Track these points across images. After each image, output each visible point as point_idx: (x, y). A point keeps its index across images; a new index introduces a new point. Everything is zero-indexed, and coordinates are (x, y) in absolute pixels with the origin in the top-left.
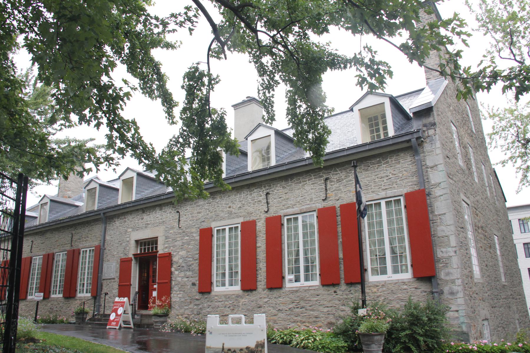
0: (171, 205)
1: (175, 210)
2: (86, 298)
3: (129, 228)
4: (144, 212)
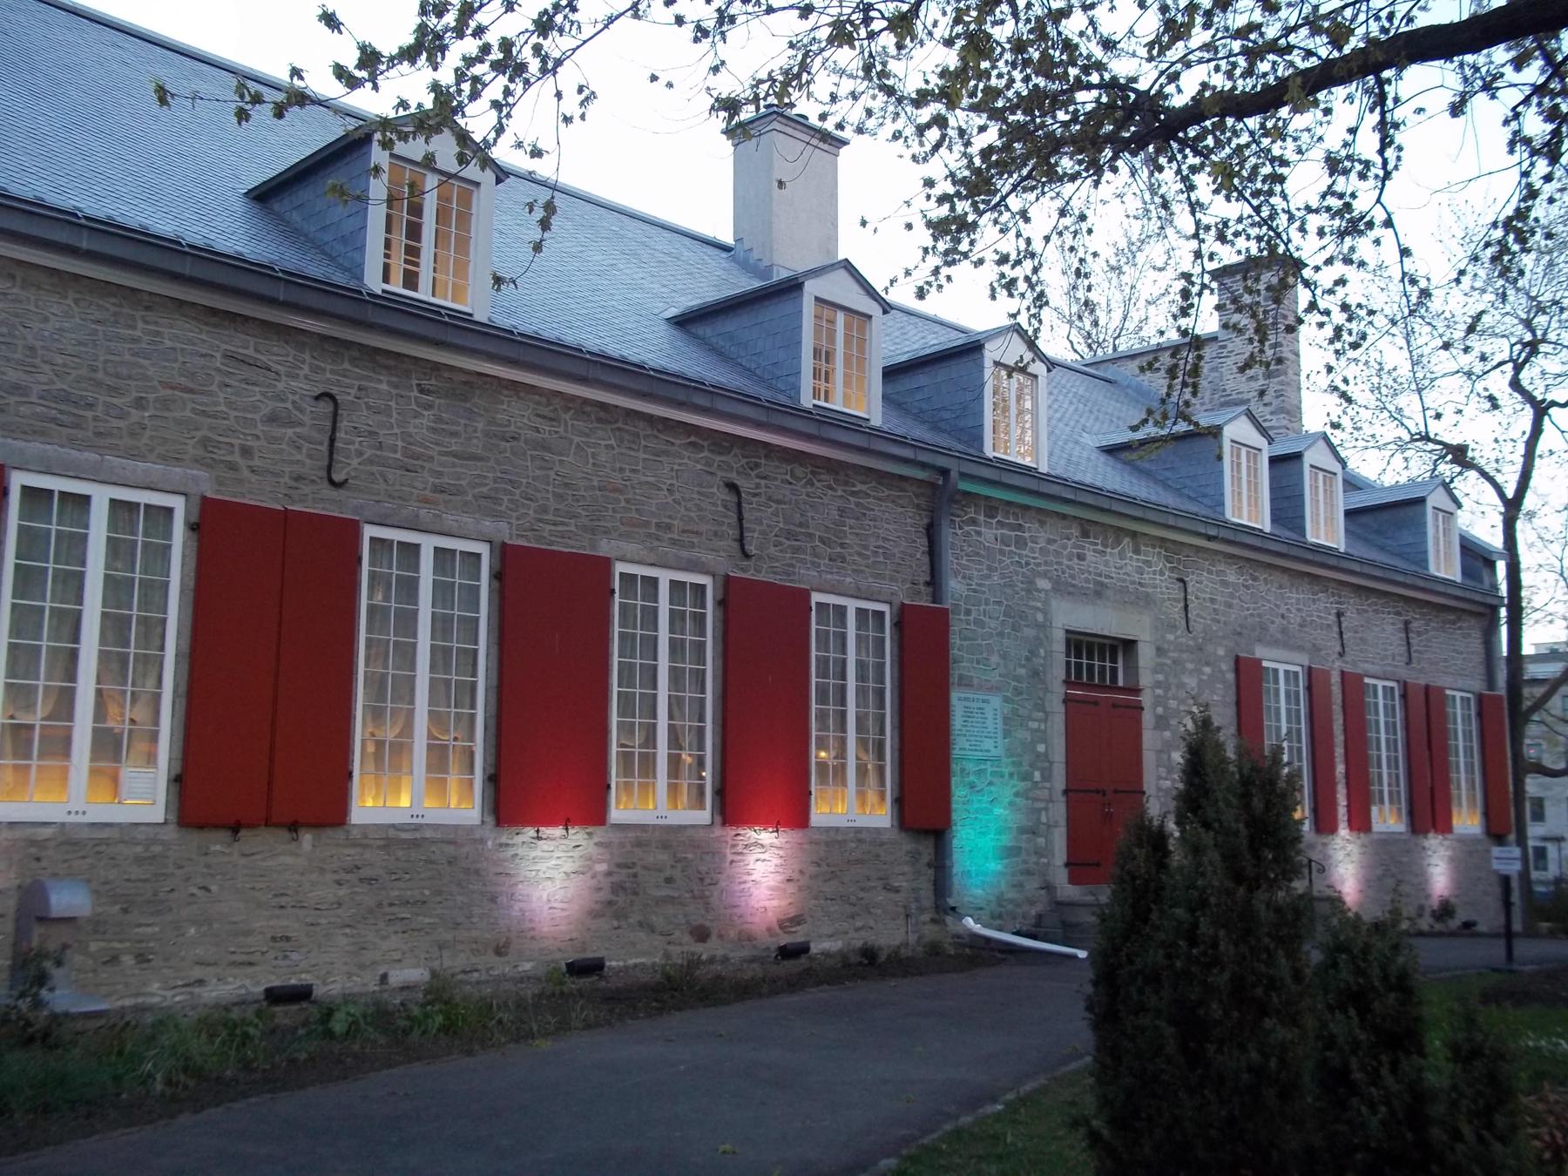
0: (1161, 547)
1: (1172, 569)
2: (863, 836)
3: (1045, 575)
4: (1085, 534)
